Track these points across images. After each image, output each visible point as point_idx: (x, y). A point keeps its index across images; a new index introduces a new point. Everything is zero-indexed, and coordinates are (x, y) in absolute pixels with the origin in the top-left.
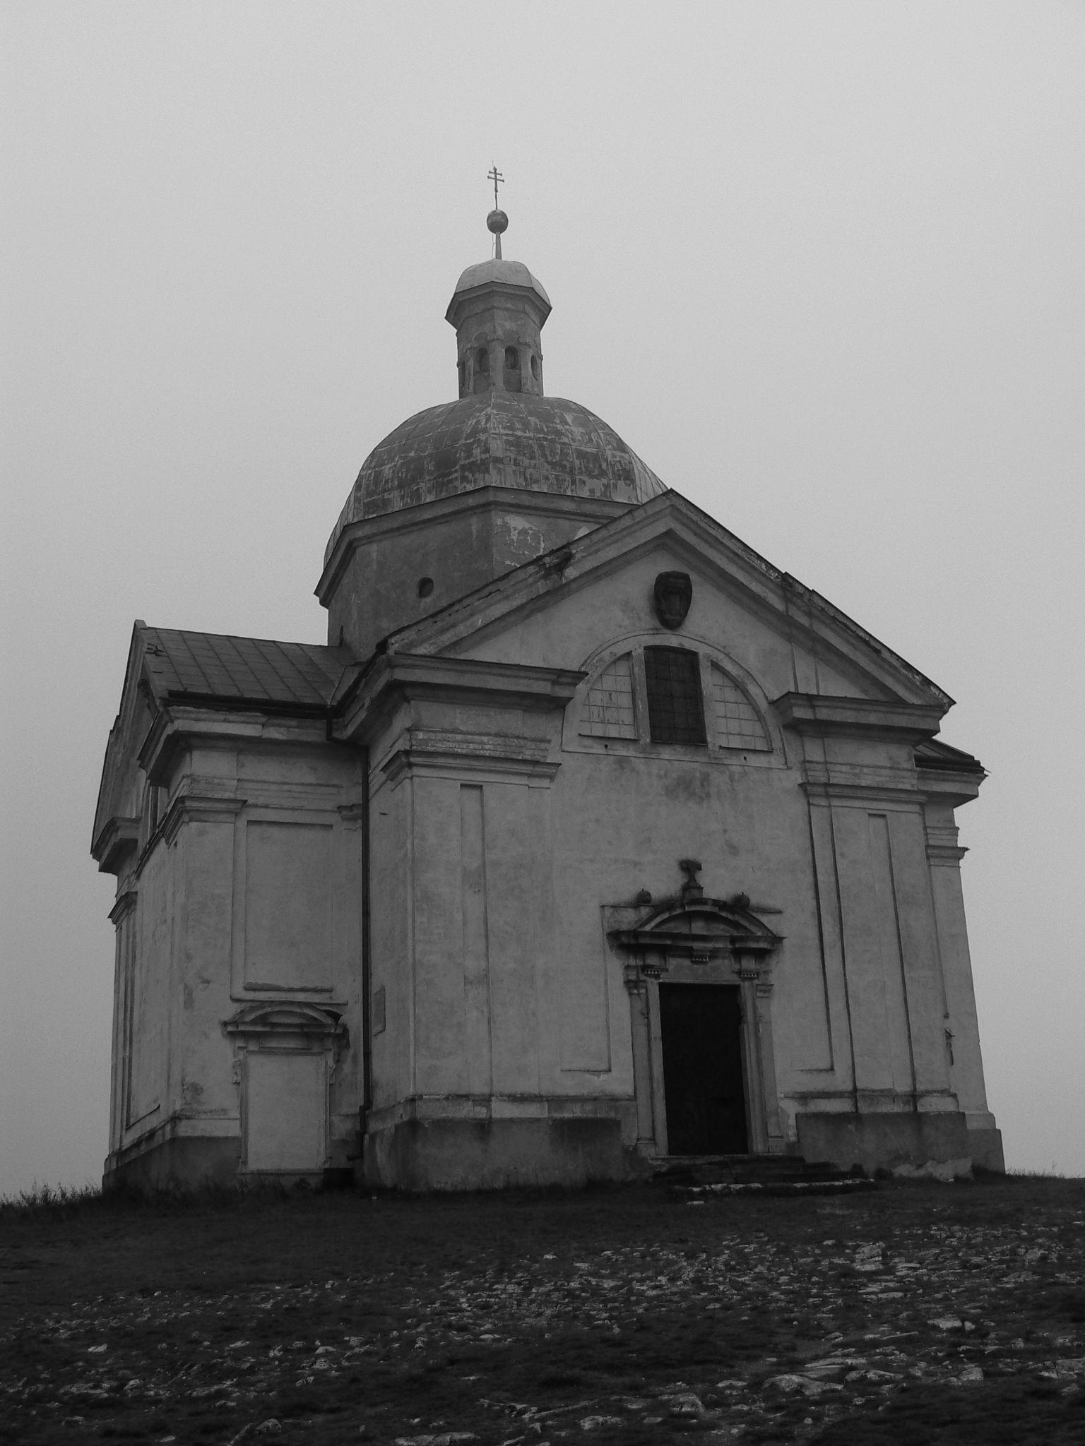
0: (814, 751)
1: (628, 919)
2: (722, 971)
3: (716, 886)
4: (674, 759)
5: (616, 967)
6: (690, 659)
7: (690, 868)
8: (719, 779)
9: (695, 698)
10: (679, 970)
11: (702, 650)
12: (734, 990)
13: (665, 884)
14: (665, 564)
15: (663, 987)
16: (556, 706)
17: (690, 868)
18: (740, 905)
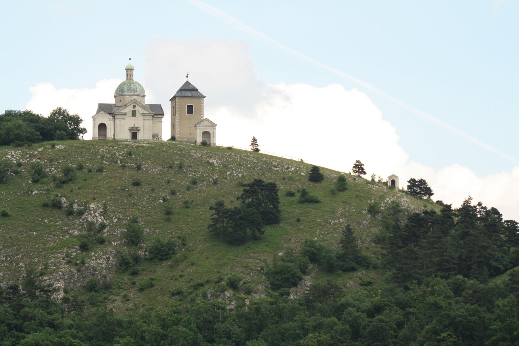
0: (144, 117)
1: (130, 128)
2: (136, 131)
3: (136, 126)
4: (134, 118)
5: (129, 131)
6: (136, 110)
7: (134, 125)
8: (137, 119)
9: (136, 113)
10: (133, 131)
11: (137, 110)
12: (136, 133)
13: (132, 126)
14: (134, 104)
15: (132, 133)
16: (126, 115)
17: (134, 125)
18: (138, 127)
